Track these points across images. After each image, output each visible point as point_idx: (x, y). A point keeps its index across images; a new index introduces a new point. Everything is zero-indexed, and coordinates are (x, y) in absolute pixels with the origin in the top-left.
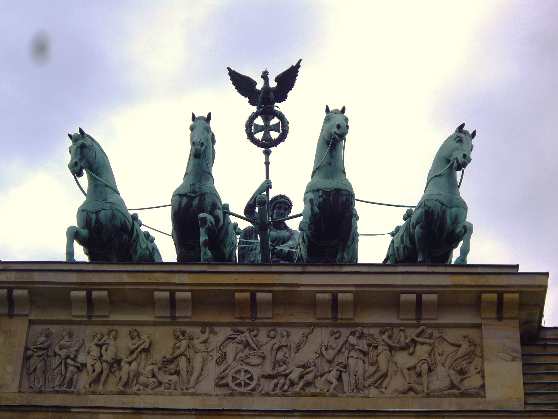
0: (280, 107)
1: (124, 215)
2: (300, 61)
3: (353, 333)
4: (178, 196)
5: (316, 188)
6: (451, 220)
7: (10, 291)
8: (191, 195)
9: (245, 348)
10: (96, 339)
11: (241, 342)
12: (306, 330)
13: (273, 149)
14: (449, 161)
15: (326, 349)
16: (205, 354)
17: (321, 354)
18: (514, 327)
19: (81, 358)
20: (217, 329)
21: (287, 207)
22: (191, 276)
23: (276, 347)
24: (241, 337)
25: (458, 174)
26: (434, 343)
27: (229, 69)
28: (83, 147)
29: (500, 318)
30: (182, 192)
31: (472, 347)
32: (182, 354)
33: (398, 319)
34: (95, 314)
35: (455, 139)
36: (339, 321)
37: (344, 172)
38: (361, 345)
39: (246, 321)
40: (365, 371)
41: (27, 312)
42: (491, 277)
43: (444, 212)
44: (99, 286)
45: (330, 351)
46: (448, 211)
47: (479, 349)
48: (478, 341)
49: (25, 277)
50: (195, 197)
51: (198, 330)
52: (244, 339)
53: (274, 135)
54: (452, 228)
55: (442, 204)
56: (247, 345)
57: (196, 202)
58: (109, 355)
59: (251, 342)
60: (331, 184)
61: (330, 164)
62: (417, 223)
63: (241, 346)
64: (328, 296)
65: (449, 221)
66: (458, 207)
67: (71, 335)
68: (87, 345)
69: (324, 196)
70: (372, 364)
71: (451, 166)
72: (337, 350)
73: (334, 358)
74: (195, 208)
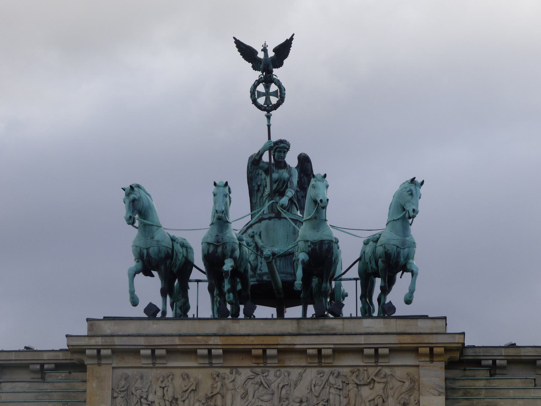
0: (277, 72)
1: (167, 247)
2: (293, 34)
3: (332, 373)
4: (206, 244)
5: (305, 239)
6: (404, 258)
7: (99, 351)
8: (215, 243)
9: (260, 386)
10: (159, 381)
11: (257, 383)
12: (300, 370)
13: (273, 113)
14: (404, 209)
15: (315, 386)
16: (233, 391)
17: (311, 389)
18: (441, 368)
19: (151, 398)
20: (240, 370)
21: (286, 150)
22: (222, 338)
23: (281, 386)
24: (258, 379)
25: (410, 221)
26: (387, 381)
27: (234, 38)
28: (134, 201)
29: (432, 361)
30: (209, 241)
31: (412, 384)
32: (218, 393)
33: (363, 362)
34: (157, 362)
35: (408, 192)
36: (323, 365)
37: (326, 220)
38: (338, 384)
39: (261, 365)
40: (340, 403)
41: (110, 362)
42: (425, 336)
43: (399, 253)
44: (160, 347)
45: (317, 388)
46: (402, 251)
47: (417, 384)
48: (417, 377)
49: (109, 341)
50: (219, 246)
51: (227, 371)
52: (259, 380)
53: (274, 100)
54: (404, 263)
55: (398, 247)
56: (262, 383)
57: (220, 250)
58: (169, 397)
59: (264, 383)
60: (315, 236)
61: (316, 218)
62: (380, 257)
63: (257, 386)
64: (315, 352)
65: (402, 259)
66: (409, 247)
67: (142, 377)
68: (154, 387)
69: (312, 246)
70: (345, 397)
71: (404, 215)
72: (322, 387)
73: (319, 394)
74: (220, 255)
